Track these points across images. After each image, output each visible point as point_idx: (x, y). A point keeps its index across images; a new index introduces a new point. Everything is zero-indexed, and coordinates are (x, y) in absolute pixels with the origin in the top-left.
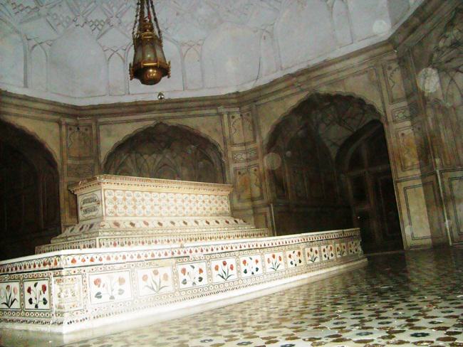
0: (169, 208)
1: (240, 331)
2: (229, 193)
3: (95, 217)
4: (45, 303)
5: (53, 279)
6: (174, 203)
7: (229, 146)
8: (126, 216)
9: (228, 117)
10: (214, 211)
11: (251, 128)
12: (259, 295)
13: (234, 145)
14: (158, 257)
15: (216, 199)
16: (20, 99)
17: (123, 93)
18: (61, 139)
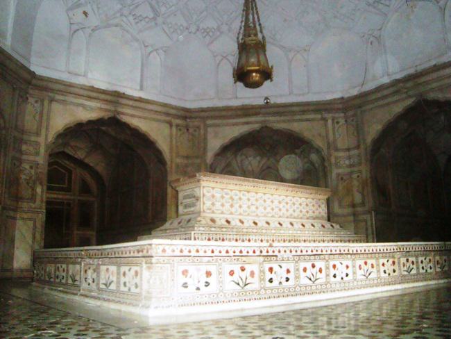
0: (265, 208)
1: (314, 333)
2: (326, 197)
3: (193, 213)
4: (137, 287)
5: (144, 266)
6: (270, 204)
7: (332, 151)
8: (222, 213)
9: (333, 123)
10: (311, 214)
11: (355, 134)
12: (346, 300)
13: (337, 150)
14: (246, 254)
15: (314, 202)
16: (136, 100)
17: (230, 96)
18: (171, 138)
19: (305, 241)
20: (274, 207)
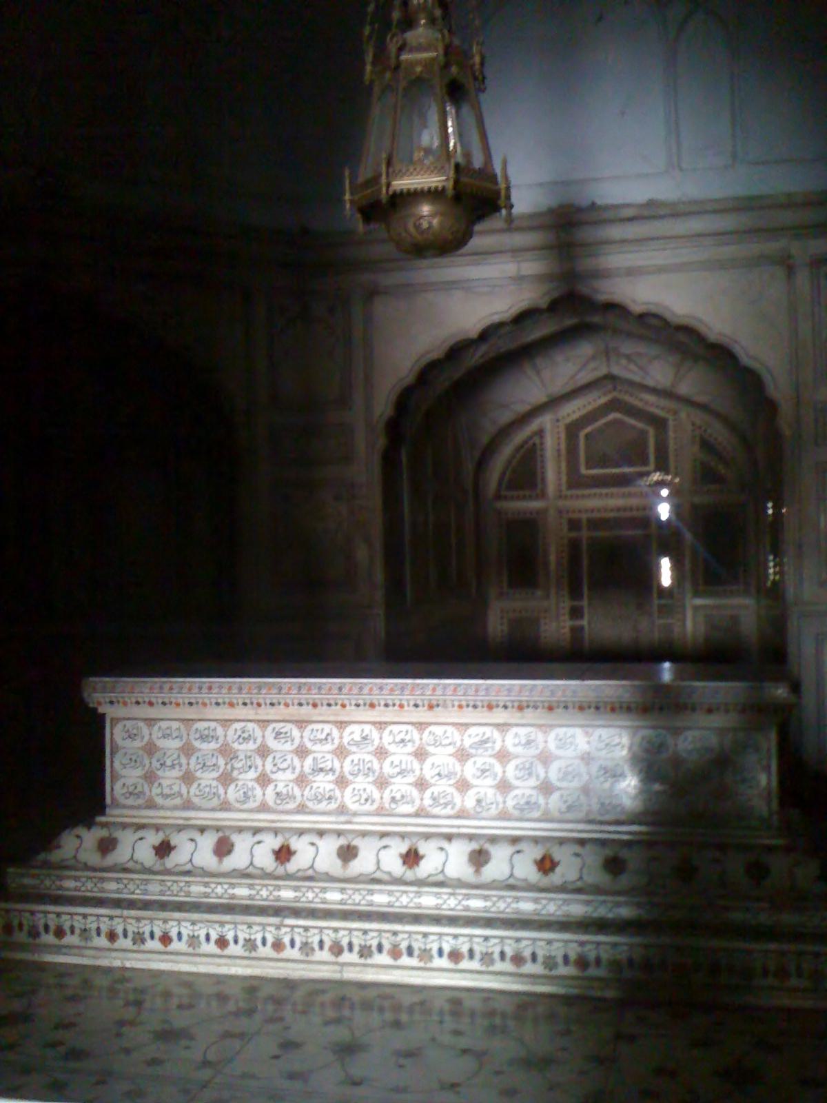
0: (382, 783)
19: (455, 956)
20: (429, 773)
